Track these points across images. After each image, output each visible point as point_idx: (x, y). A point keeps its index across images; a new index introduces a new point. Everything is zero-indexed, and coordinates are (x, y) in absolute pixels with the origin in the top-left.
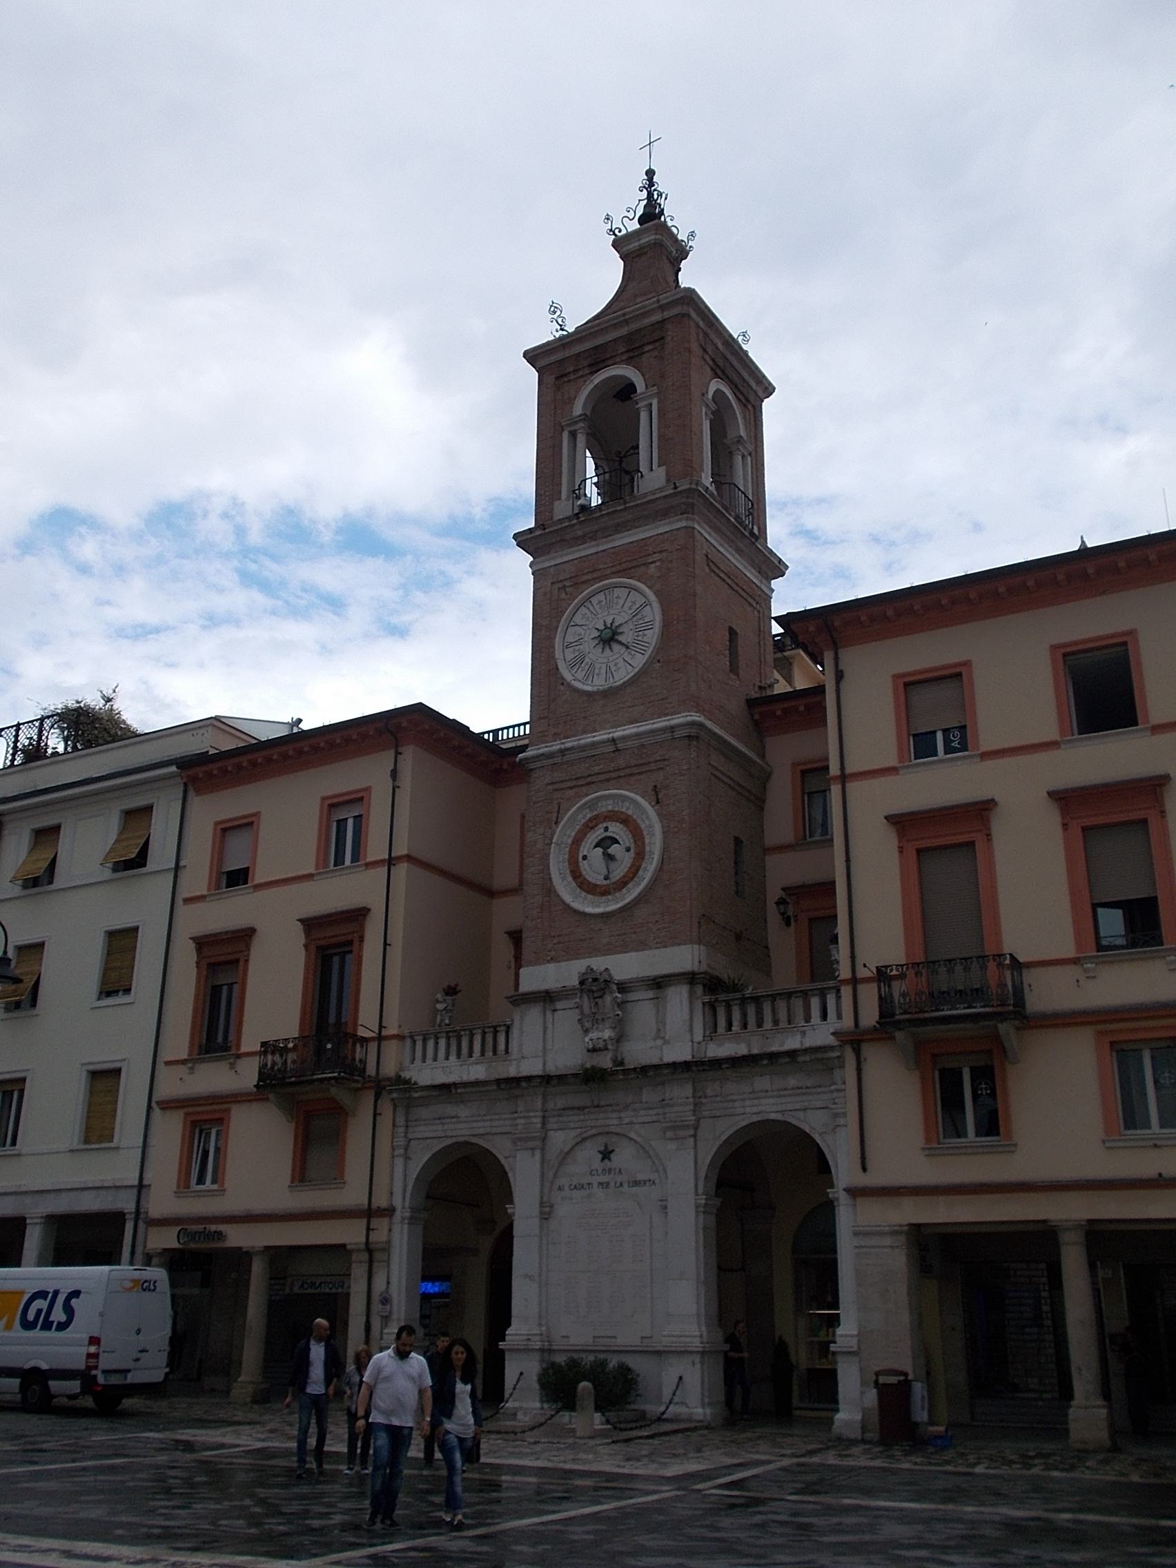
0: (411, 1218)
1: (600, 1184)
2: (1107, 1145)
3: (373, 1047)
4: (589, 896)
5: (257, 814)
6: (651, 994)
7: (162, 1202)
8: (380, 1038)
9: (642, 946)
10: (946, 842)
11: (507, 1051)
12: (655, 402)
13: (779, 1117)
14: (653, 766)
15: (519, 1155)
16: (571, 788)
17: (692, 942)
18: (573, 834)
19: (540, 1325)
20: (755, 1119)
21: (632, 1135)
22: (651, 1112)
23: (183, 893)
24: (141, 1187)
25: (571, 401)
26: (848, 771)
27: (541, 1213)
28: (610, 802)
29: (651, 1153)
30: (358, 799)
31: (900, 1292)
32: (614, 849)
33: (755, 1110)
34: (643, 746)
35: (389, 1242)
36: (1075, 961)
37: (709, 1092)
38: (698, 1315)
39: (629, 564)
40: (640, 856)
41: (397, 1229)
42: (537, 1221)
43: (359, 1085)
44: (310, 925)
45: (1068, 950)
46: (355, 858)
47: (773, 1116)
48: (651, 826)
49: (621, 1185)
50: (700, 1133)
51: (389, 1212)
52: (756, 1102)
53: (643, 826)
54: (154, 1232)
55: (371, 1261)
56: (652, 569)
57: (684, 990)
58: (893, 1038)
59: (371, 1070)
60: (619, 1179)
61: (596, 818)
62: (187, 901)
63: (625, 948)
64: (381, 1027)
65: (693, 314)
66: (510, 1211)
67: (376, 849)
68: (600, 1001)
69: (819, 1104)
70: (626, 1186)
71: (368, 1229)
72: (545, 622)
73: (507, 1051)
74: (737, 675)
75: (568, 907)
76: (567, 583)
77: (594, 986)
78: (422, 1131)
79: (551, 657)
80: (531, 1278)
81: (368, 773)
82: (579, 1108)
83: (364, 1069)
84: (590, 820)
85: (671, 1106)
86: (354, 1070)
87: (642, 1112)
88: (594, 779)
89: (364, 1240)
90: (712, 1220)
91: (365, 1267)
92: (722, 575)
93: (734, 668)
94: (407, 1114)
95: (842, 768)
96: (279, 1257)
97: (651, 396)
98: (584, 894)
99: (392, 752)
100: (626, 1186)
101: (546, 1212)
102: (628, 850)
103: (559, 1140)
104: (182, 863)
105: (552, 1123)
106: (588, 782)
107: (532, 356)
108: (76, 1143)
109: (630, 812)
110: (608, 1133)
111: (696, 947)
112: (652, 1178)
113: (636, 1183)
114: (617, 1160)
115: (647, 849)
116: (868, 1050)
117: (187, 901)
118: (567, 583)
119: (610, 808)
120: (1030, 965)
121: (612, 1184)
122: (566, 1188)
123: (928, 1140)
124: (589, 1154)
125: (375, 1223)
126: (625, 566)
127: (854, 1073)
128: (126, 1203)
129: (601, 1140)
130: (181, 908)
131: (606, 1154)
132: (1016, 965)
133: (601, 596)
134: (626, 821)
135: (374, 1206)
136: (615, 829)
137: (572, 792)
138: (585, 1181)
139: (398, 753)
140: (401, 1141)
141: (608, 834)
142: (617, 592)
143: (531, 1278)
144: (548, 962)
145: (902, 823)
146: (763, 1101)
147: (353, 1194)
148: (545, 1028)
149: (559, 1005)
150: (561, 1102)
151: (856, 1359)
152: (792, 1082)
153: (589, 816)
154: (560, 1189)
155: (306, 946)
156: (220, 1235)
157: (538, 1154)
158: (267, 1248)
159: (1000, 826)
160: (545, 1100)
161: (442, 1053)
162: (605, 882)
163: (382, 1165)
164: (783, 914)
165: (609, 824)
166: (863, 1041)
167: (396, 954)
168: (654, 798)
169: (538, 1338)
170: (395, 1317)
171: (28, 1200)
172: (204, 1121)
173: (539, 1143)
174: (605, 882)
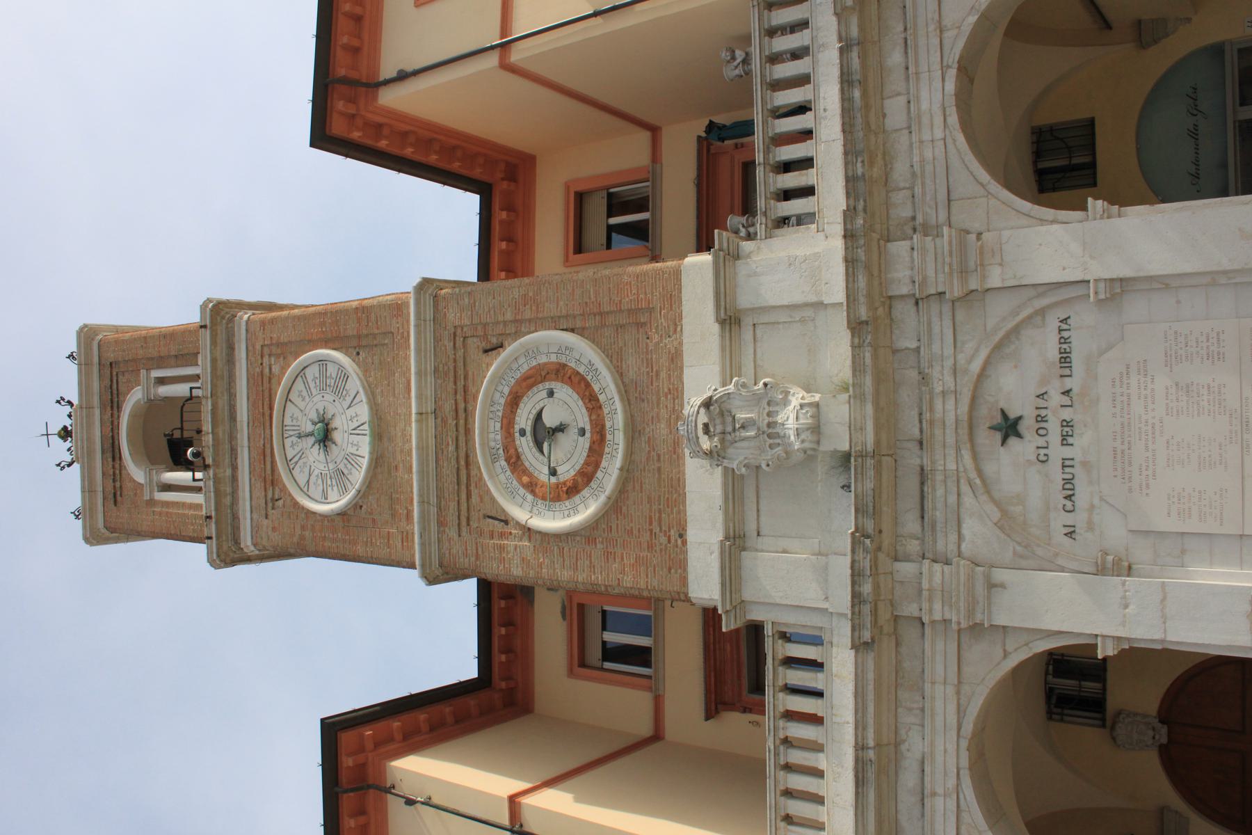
1: (1065, 440)
4: (604, 464)
6: (747, 335)
9: (676, 358)
11: (816, 641)
13: (952, 73)
14: (460, 353)
18: (522, 491)
20: (953, 119)
21: (976, 366)
22: (936, 329)
28: (492, 423)
29: (1010, 325)
32: (549, 420)
33: (938, 120)
34: (436, 370)
37: (906, 213)
47: (950, 86)
48: (526, 353)
49: (1067, 393)
52: (925, 120)
53: (526, 367)
60: (1056, 398)
61: (506, 449)
63: (676, 393)
70: (1068, 383)
76: (270, 495)
84: (508, 460)
85: (925, 279)
87: (936, 347)
97: (148, 377)
98: (599, 474)
100: (1068, 383)
102: (551, 394)
105: (944, 544)
109: (506, 390)
110: (971, 428)
112: (1053, 323)
113: (1065, 359)
115: (553, 358)
118: (270, 495)
119: (498, 425)
121: (1066, 414)
122: (1069, 519)
124: (1009, 464)
126: (266, 407)
131: (1009, 428)
133: (288, 442)
137: (475, 499)
138: (1058, 477)
139: (389, 790)
141: (529, 430)
142: (288, 421)
144: (684, 543)
146: (925, 106)
149: (751, 527)
152: (895, 58)
153: (503, 463)
154: (1070, 535)
162: (588, 435)
165: (517, 428)
174: (588, 435)
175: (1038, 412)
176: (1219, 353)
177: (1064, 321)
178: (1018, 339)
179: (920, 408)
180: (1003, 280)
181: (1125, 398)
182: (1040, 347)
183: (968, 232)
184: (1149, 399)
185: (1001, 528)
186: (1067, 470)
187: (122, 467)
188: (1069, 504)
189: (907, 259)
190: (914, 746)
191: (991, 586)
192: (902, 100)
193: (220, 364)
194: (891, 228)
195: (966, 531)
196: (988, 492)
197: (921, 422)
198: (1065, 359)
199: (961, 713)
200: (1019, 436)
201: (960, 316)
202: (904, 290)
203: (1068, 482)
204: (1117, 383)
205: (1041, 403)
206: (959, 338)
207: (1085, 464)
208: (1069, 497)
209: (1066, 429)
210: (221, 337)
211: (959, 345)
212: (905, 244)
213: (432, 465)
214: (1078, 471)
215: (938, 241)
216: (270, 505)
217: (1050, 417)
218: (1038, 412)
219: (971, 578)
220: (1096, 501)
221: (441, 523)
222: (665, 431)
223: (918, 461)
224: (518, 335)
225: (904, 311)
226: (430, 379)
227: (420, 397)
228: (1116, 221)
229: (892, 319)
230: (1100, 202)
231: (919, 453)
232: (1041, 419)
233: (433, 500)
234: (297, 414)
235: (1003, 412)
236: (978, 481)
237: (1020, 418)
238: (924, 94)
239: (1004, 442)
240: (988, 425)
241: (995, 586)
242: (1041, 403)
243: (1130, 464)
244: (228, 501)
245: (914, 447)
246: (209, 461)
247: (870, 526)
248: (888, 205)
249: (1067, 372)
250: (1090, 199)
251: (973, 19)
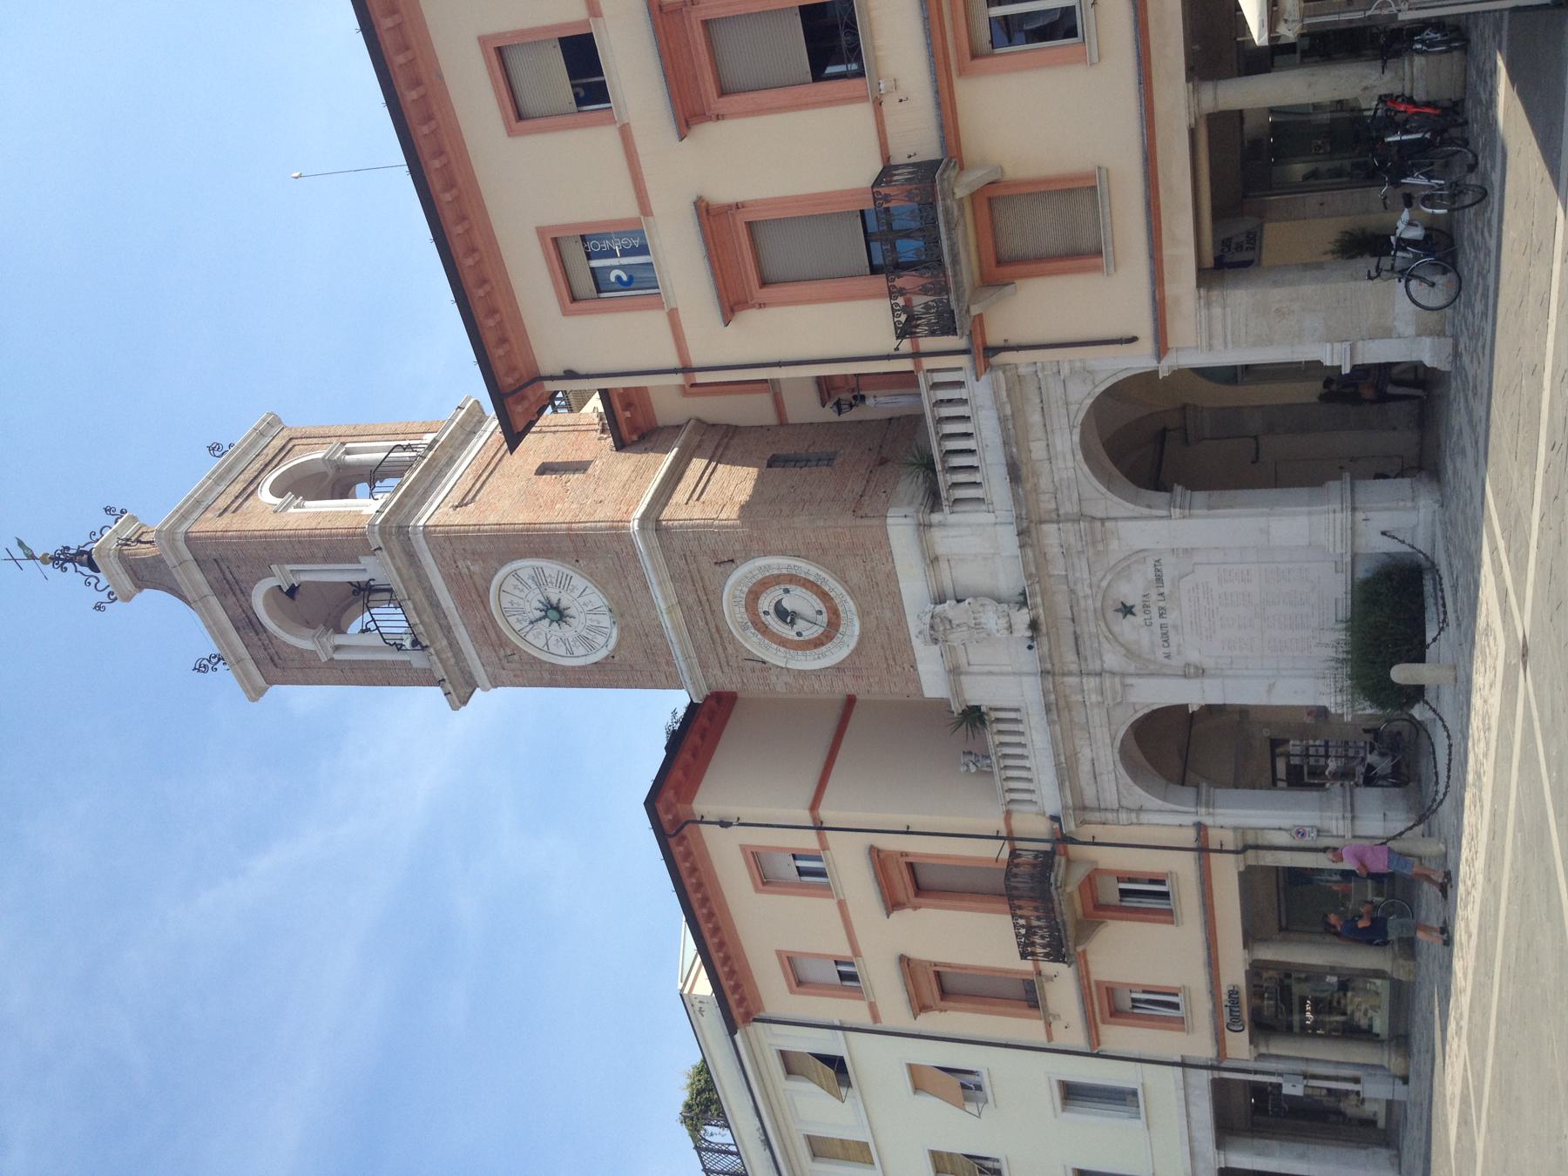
0: (1207, 806)
1: (1161, 615)
2: (1095, 59)
3: (1019, 845)
5: (779, 953)
6: (944, 565)
7: (1200, 1045)
8: (1010, 838)
9: (892, 576)
10: (747, 254)
11: (1017, 710)
12: (289, 567)
13: (1077, 431)
15: (1132, 699)
16: (725, 649)
17: (885, 526)
20: (1080, 456)
21: (1104, 584)
23: (867, 1022)
24: (1183, 1064)
25: (301, 652)
26: (673, 361)
27: (1196, 676)
30: (756, 858)
31: (1277, 295)
33: (1069, 456)
35: (1235, 829)
36: (878, 104)
38: (1310, 513)
39: (474, 596)
40: (793, 579)
41: (1220, 821)
42: (1207, 682)
43: (1063, 860)
44: (892, 904)
45: (864, 111)
46: (819, 859)
47: (1076, 438)
50: (1099, 514)
51: (1200, 828)
53: (760, 577)
54: (1230, 1053)
55: (1257, 847)
56: (475, 568)
57: (937, 534)
58: (980, 316)
59: (1047, 847)
60: (1154, 597)
62: (876, 1017)
63: (897, 595)
64: (997, 838)
65: (183, 528)
66: (1196, 708)
67: (808, 841)
68: (955, 622)
69: (1060, 390)
71: (1221, 851)
72: (547, 676)
73: (1017, 710)
74: (590, 463)
75: (857, 651)
77: (937, 631)
78: (1110, 797)
79: (583, 669)
80: (1271, 687)
81: (725, 853)
82: (1076, 639)
83: (1045, 853)
86: (1045, 862)
88: (712, 626)
89: (1231, 857)
90: (1200, 496)
91: (1262, 853)
92: (478, 485)
93: (580, 467)
94: (1092, 809)
95: (675, 371)
96: (1251, 937)
99: (702, 826)
103: (1112, 659)
104: (837, 1023)
106: (719, 634)
107: (255, 694)
108: (1139, 1124)
111: (889, 521)
113: (1159, 579)
114: (1133, 599)
116: (994, 337)
117: (876, 1017)
120: (886, 157)
121: (1162, 604)
123: (1098, 268)
124: (1127, 628)
125: (1214, 844)
127: (1022, 353)
128: (1203, 1079)
129: (1110, 614)
130: (886, 1024)
131: (1127, 610)
132: (887, 172)
133: (512, 620)
134: (754, 595)
135: (1194, 845)
136: (766, 603)
137: (730, 650)
140: (1123, 816)
141: (772, 611)
143: (1271, 687)
145: (731, 304)
146: (1059, 448)
147: (1183, 868)
148: (990, 673)
149: (963, 661)
151: (1360, 344)
152: (1035, 418)
155: (915, 908)
156: (1233, 994)
157: (1129, 681)
158: (1246, 946)
159: (722, 194)
160: (1070, 674)
161: (1024, 774)
163: (1150, 830)
164: (851, 406)
166: (984, 342)
167: (918, 821)
168: (728, 566)
170: (1317, 823)
171: (1201, 1166)
172: (1110, 1005)
173: (1117, 680)
187: (271, 637)
190: (1085, 754)
192: (1043, 444)
193: (404, 571)
199: (1113, 739)
203: (1165, 634)
207: (1175, 627)
210: (397, 548)
213: (686, 634)
216: (504, 662)
221: (704, 666)
222: (888, 614)
224: (748, 558)
226: (670, 585)
227: (665, 598)
233: (693, 654)
234: (516, 600)
238: (1058, 442)
244: (452, 661)
246: (426, 642)
247: (1049, 666)
251: (1089, 401)
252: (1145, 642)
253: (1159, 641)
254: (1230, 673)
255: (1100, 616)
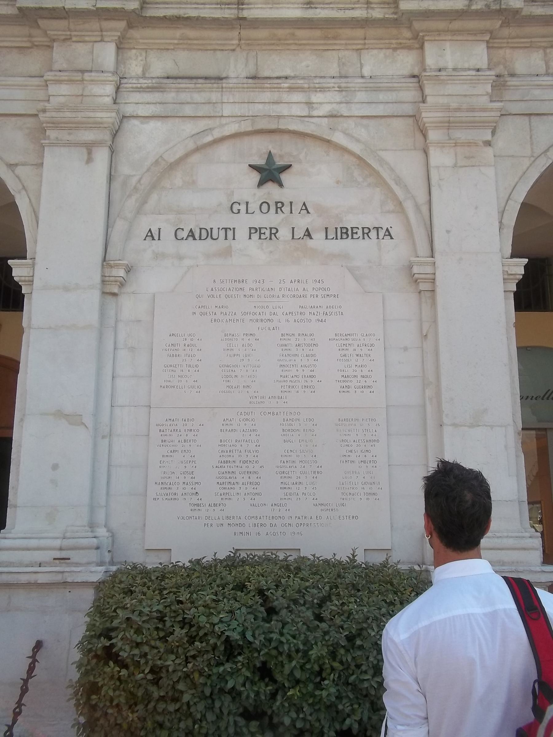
1: (253, 231)
19: (92, 526)
21: (339, 138)
22: (382, 97)
29: (385, 175)
42: (96, 295)
49: (308, 234)
60: (302, 222)
70: (319, 236)
80: (74, 419)
87: (361, 96)
100: (319, 236)
101: (113, 283)
105: (136, 103)
113: (345, 233)
114: (293, 186)
121: (284, 233)
131: (270, 173)
143: (74, 419)
150: (161, 65)
154: (150, 235)
157: (102, 156)
169: (93, 556)
173: (107, 136)
175: (287, 204)
176: (348, 387)
177: (388, 233)
178: (369, 185)
179: (294, 77)
180: (438, 167)
181: (301, 292)
182: (359, 206)
183: (493, 133)
184: (299, 317)
185: (157, 162)
186: (222, 233)
188: (185, 234)
189: (466, 66)
191: (89, 147)
194: (501, 52)
195: (153, 124)
196: (197, 149)
197: (278, 78)
198: (345, 233)
200: (261, 183)
201: (397, 123)
202: (430, 61)
204: (318, 285)
205: (297, 208)
206: (372, 122)
207: (227, 253)
208: (191, 234)
209: (268, 233)
211: (365, 121)
212: (483, 62)
214: (221, 243)
215: (486, 99)
217: (281, 216)
218: (287, 204)
219: (97, 125)
220: (187, 262)
223: (232, 75)
225: (406, 62)
228: (500, 287)
229: (395, 49)
230: (521, 271)
231: (244, 74)
232: (279, 206)
235: (288, 167)
236: (209, 138)
237: (281, 185)
239: (253, 167)
240: (272, 151)
241: (90, 153)
242: (297, 208)
243: (227, 296)
245: (251, 70)
248: (531, 47)
249: (331, 235)
250: (526, 261)
252: (190, 199)
253: (190, 223)
254: (110, 346)
255: (262, 124)
